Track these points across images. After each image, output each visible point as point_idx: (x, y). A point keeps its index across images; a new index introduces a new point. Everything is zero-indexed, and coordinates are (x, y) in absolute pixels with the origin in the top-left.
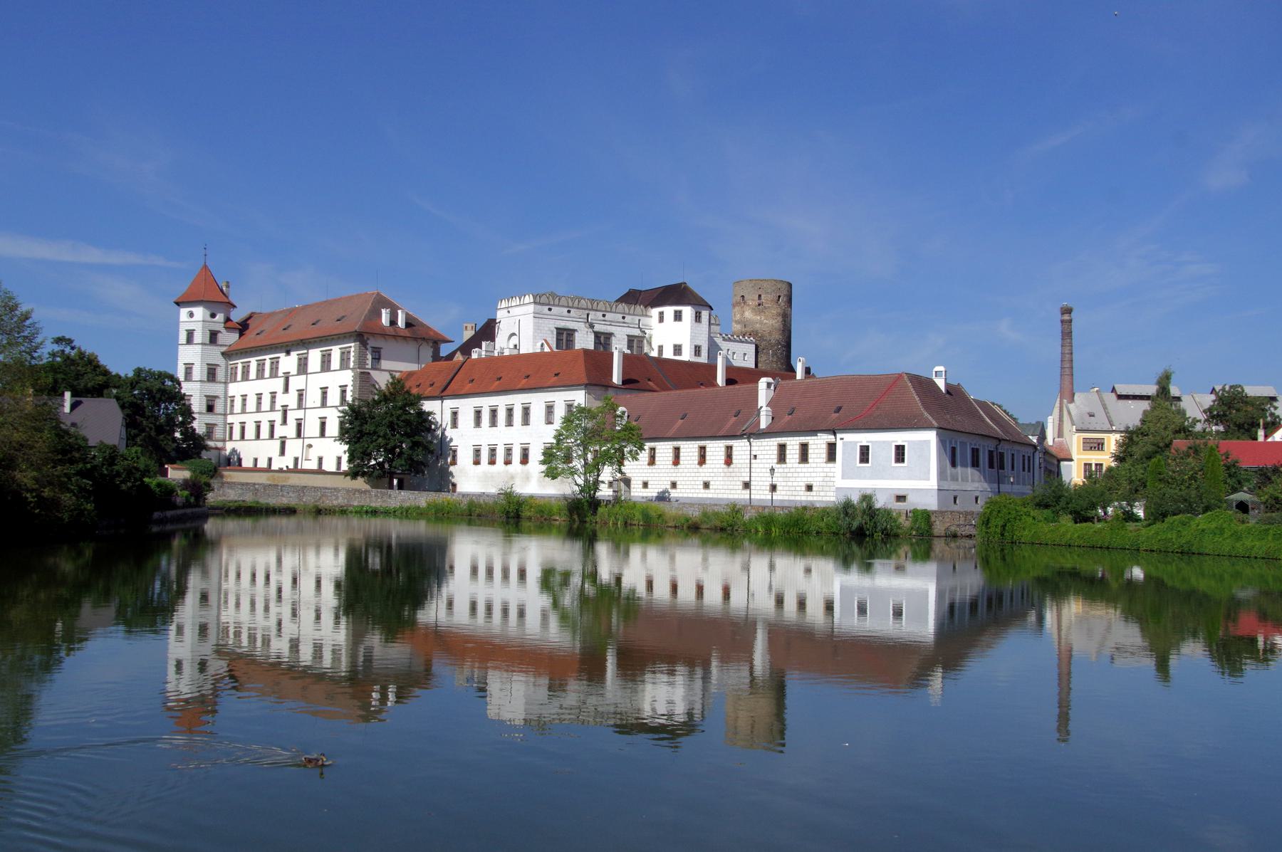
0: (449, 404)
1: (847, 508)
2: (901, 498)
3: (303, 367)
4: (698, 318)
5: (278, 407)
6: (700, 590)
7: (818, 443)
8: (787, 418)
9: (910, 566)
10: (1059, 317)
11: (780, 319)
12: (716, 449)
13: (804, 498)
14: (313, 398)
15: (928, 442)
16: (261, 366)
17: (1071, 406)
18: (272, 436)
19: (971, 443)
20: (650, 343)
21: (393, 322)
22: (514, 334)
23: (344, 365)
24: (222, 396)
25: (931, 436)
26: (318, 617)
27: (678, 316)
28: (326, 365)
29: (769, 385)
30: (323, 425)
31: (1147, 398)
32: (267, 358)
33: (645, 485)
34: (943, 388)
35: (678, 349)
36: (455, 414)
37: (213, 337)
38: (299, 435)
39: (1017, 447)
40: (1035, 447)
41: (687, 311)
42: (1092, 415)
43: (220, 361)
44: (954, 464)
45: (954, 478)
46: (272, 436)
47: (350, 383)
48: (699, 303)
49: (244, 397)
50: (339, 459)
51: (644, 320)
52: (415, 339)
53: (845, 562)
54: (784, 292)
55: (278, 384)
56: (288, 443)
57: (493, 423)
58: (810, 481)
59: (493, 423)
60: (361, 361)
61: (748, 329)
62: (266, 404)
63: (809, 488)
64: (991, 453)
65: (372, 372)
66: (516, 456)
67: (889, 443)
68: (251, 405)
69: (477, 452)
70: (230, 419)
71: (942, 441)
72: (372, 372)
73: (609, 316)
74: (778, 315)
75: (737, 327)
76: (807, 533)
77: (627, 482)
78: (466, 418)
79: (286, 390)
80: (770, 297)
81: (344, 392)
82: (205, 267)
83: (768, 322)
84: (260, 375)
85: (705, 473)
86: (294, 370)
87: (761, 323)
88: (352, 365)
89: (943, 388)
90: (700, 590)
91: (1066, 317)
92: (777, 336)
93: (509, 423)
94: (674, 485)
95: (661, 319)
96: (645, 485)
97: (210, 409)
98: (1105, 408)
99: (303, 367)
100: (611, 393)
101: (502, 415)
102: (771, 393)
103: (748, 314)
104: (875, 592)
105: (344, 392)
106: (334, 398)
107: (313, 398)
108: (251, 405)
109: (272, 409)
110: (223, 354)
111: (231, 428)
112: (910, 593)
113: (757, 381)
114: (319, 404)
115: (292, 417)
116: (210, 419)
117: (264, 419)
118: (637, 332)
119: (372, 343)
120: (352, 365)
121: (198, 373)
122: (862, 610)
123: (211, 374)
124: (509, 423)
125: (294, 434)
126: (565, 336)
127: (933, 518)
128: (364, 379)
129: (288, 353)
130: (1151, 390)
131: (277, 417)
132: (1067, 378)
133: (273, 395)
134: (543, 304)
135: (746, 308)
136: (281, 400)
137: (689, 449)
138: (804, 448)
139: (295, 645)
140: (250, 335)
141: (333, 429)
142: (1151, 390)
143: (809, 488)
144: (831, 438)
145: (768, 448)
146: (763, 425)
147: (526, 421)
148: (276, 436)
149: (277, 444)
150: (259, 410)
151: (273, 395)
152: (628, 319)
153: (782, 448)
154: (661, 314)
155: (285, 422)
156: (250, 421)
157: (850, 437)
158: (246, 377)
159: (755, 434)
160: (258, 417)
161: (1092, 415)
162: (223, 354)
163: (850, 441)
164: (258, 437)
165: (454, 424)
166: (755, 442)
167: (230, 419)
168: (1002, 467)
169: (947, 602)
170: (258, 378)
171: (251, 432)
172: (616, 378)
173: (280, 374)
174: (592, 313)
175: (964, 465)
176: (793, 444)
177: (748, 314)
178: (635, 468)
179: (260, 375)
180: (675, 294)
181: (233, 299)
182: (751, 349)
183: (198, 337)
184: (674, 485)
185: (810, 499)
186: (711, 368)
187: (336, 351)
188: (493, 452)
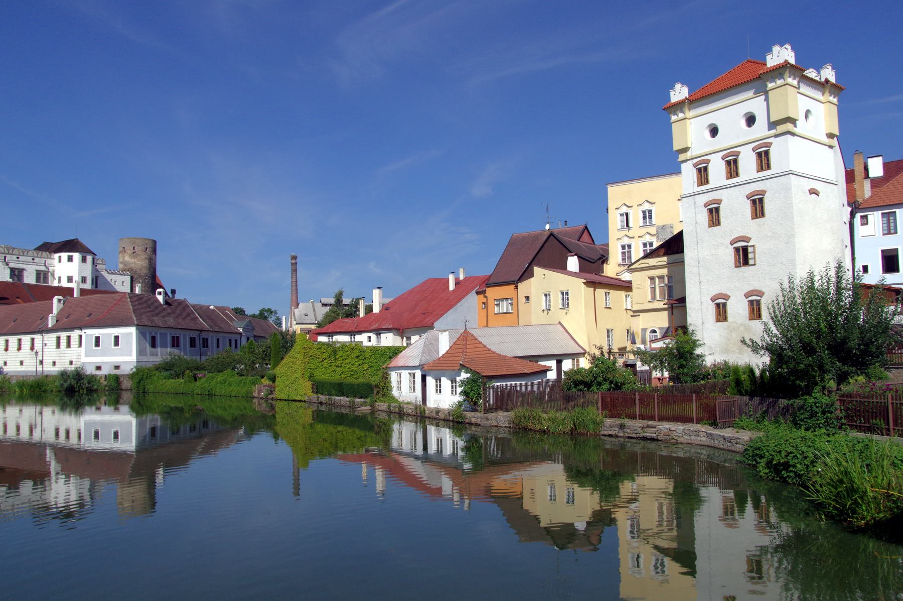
1: (64, 374)
2: (117, 367)
4: (84, 260)
6: (18, 428)
9: (105, 408)
10: (290, 261)
12: (26, 339)
15: (131, 334)
17: (296, 311)
20: (53, 275)
25: (132, 330)
27: (70, 259)
29: (59, 301)
31: (330, 305)
35: (70, 279)
39: (221, 335)
40: (241, 334)
41: (77, 256)
42: (306, 315)
44: (153, 345)
45: (152, 354)
48: (84, 251)
51: (48, 261)
53: (63, 408)
54: (150, 245)
71: (141, 334)
73: (22, 258)
75: (121, 266)
76: (45, 391)
83: (140, 263)
90: (18, 428)
91: (294, 261)
92: (145, 271)
94: (5, 363)
95: (60, 261)
98: (314, 310)
102: (61, 305)
103: (127, 258)
104: (103, 424)
112: (121, 424)
113: (52, 299)
118: (43, 268)
122: (97, 436)
127: (122, 379)
130: (332, 301)
132: (294, 295)
137: (13, 340)
138: (69, 338)
142: (332, 301)
145: (51, 338)
146: (50, 326)
152: (37, 260)
153: (59, 338)
161: (306, 315)
166: (46, 336)
169: (148, 427)
175: (164, 346)
176: (63, 335)
177: (127, 258)
180: (70, 246)
182: (127, 279)
184: (5, 363)
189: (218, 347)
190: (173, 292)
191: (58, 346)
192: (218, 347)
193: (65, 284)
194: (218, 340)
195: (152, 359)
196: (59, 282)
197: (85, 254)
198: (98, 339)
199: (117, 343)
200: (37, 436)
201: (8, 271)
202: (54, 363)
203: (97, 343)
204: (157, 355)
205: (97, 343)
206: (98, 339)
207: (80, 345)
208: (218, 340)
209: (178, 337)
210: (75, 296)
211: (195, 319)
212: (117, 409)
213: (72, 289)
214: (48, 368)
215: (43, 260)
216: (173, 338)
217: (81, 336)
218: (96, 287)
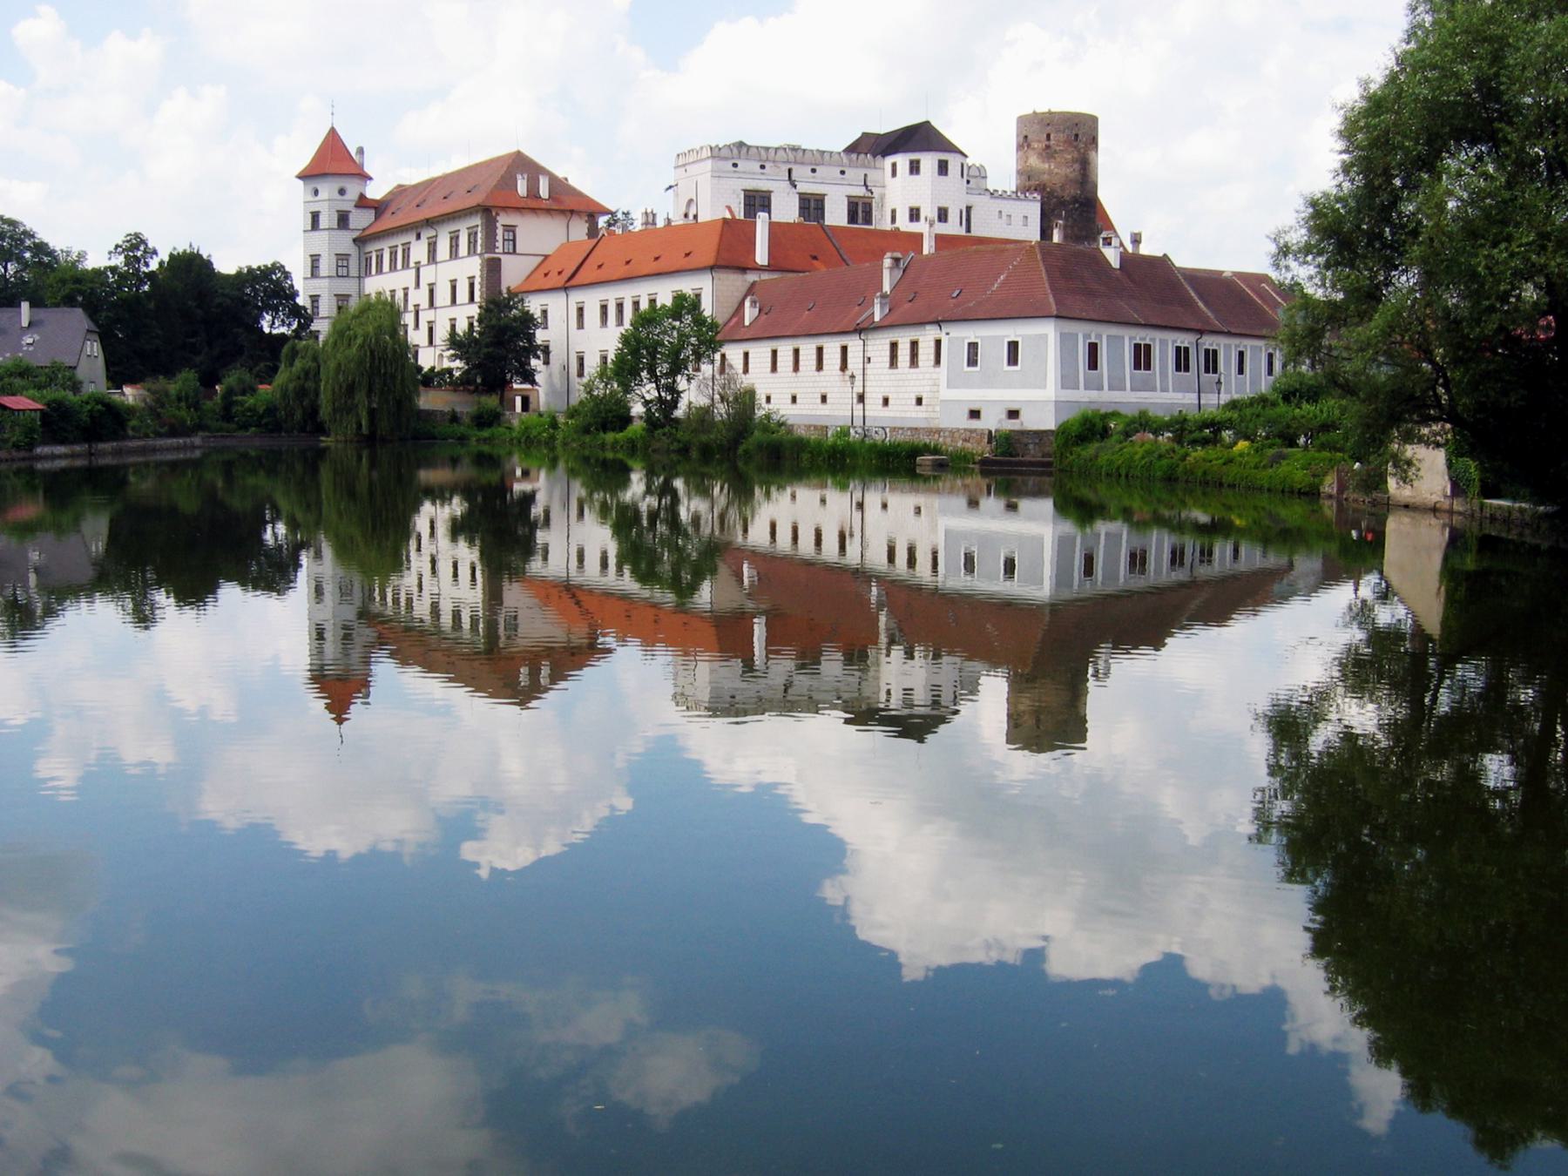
0: (576, 297)
2: (1014, 414)
4: (943, 168)
7: (927, 337)
11: (1077, 166)
12: (832, 347)
14: (443, 296)
19: (1130, 337)
21: (533, 193)
22: (691, 201)
26: (455, 575)
27: (915, 168)
28: (454, 253)
29: (897, 260)
32: (399, 241)
34: (1115, 263)
35: (915, 215)
36: (580, 311)
37: (343, 220)
41: (928, 161)
43: (352, 250)
47: (478, 274)
52: (562, 212)
55: (407, 277)
60: (490, 244)
61: (1033, 183)
63: (919, 401)
74: (1074, 161)
78: (592, 315)
80: (1062, 136)
81: (472, 286)
82: (333, 133)
84: (393, 268)
86: (424, 261)
88: (479, 250)
89: (1115, 263)
95: (894, 173)
100: (752, 277)
104: (987, 539)
105: (472, 286)
106: (463, 295)
107: (443, 296)
112: (1020, 539)
113: (882, 258)
115: (425, 317)
118: (861, 192)
119: (503, 219)
126: (757, 201)
128: (493, 269)
129: (418, 237)
134: (726, 159)
135: (1031, 152)
137: (808, 348)
138: (914, 344)
139: (435, 610)
140: (388, 215)
143: (919, 401)
145: (878, 346)
146: (877, 318)
153: (894, 346)
154: (894, 165)
155: (417, 326)
158: (380, 271)
159: (863, 329)
163: (958, 336)
165: (581, 325)
173: (412, 264)
176: (904, 339)
179: (393, 268)
181: (368, 169)
183: (324, 222)
187: (463, 228)
189: (1241, 371)
190: (1136, 240)
191: (893, 361)
192: (1241, 371)
193: (903, 224)
194: (1241, 354)
195: (1093, 395)
196: (893, 220)
197: (944, 156)
198: (973, 347)
199: (1013, 359)
200: (853, 556)
201: (795, 203)
202: (886, 401)
204: (1100, 388)
205: (972, 361)
206: (973, 347)
207: (938, 361)
208: (1241, 354)
209: (1148, 347)
210: (926, 252)
211: (1187, 303)
212: (1012, 507)
213: (918, 238)
214: (874, 409)
215: (861, 172)
216: (1137, 347)
217: (938, 343)
218: (968, 230)
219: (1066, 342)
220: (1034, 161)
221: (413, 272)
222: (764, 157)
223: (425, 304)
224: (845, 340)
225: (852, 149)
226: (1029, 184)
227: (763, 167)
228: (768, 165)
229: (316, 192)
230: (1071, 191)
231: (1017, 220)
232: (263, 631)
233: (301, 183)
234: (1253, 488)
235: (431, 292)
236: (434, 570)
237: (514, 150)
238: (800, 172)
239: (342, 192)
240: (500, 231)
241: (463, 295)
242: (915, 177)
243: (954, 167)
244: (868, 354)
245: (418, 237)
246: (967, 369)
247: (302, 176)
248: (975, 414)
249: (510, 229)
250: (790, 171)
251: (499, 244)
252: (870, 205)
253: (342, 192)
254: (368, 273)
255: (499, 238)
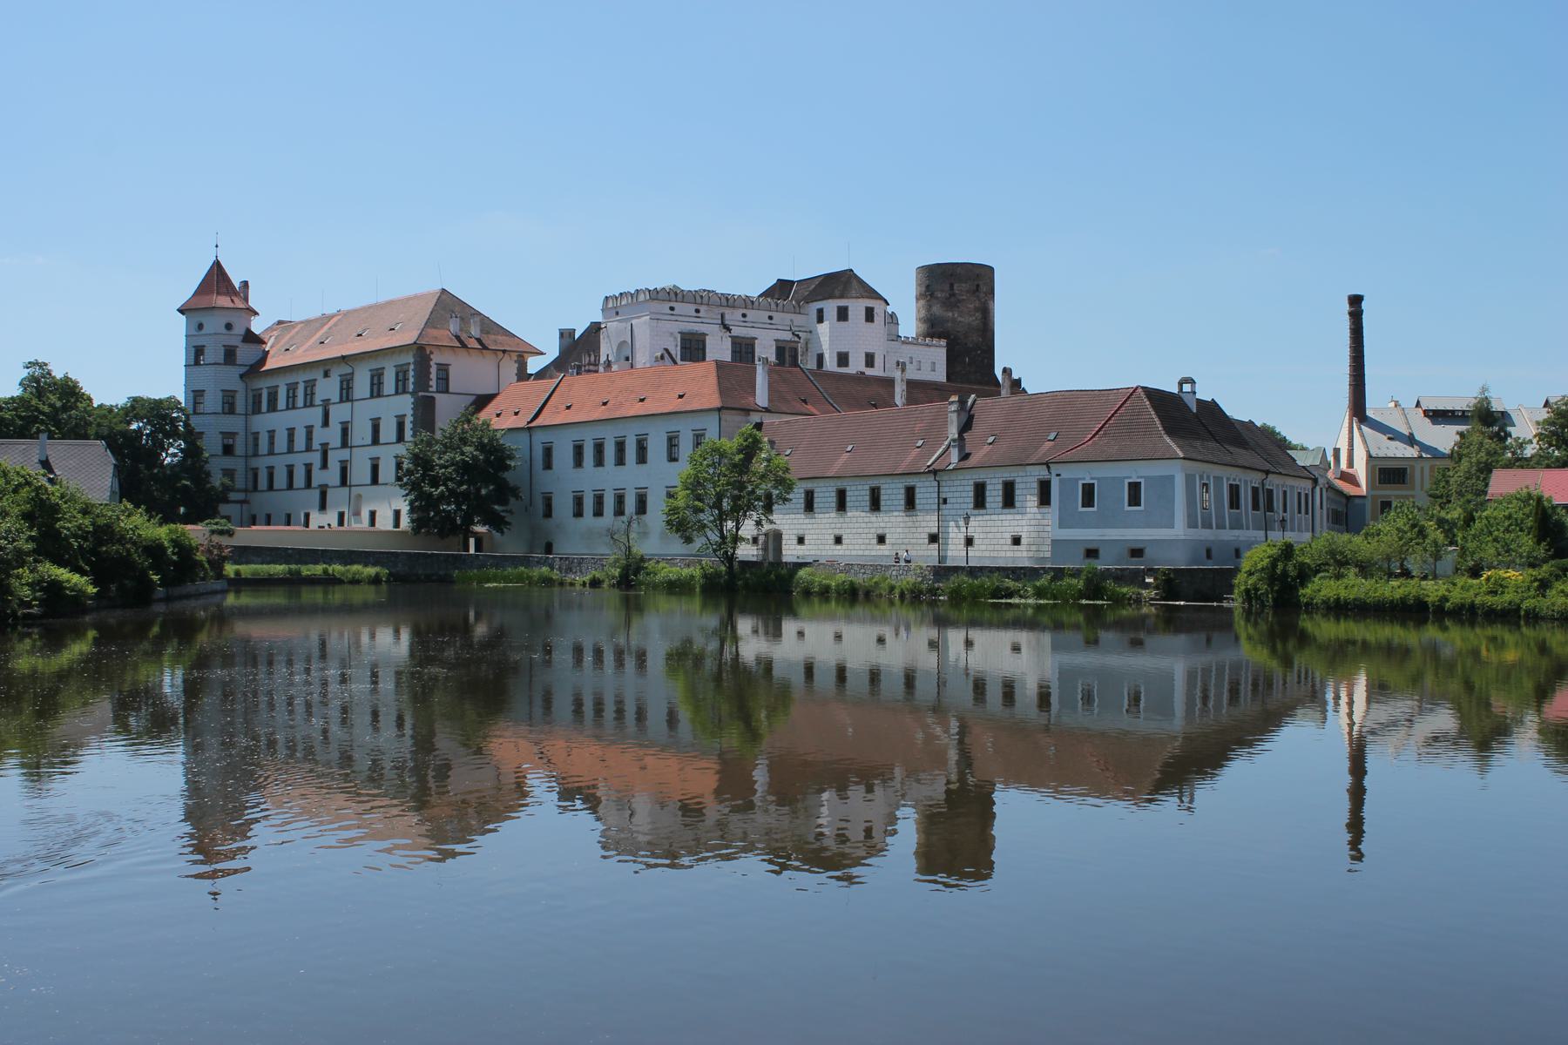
3: (346, 394)
4: (870, 315)
5: (316, 445)
8: (987, 448)
11: (978, 315)
13: (1009, 554)
14: (362, 433)
16: (292, 388)
18: (308, 485)
23: (401, 389)
24: (242, 433)
27: (843, 314)
28: (376, 391)
30: (375, 469)
33: (801, 540)
35: (843, 359)
37: (230, 355)
38: (344, 482)
41: (857, 307)
46: (308, 485)
47: (409, 412)
49: (272, 434)
50: (397, 514)
51: (798, 320)
56: (330, 493)
57: (599, 462)
58: (1017, 531)
59: (599, 462)
62: (300, 442)
63: (1016, 541)
64: (1255, 490)
65: (437, 396)
66: (630, 504)
67: (1122, 480)
68: (281, 443)
69: (579, 501)
70: (254, 463)
72: (437, 396)
74: (976, 309)
77: (777, 537)
79: (326, 423)
84: (291, 406)
85: (880, 522)
87: (954, 320)
93: (620, 461)
96: (801, 540)
97: (228, 450)
99: (346, 394)
100: (755, 418)
101: (610, 452)
106: (388, 432)
107: (362, 433)
108: (281, 443)
109: (309, 449)
110: (242, 376)
111: (256, 476)
114: (369, 440)
115: (335, 458)
116: (228, 462)
117: (299, 461)
118: (787, 336)
120: (411, 387)
121: (212, 402)
123: (229, 407)
124: (620, 461)
125: (337, 480)
129: (326, 375)
131: (315, 458)
133: (309, 431)
136: (320, 436)
141: (387, 472)
143: (1016, 541)
144: (1042, 472)
147: (642, 458)
148: (315, 483)
149: (316, 494)
150: (290, 450)
151: (309, 431)
156: (280, 464)
157: (1068, 472)
158: (273, 407)
160: (290, 459)
162: (242, 376)
164: (290, 486)
165: (548, 465)
167: (254, 463)
168: (1270, 507)
170: (288, 408)
171: (280, 480)
172: (761, 397)
173: (317, 401)
174: (727, 312)
178: (787, 521)
183: (209, 356)
185: (1018, 554)
186: (890, 382)
188: (599, 501)
198: (1088, 491)
199: (1135, 500)
201: (727, 346)
203: (1088, 499)
204: (1210, 527)
205: (1088, 499)
206: (1088, 491)
213: (890, 382)
219: (1189, 480)
220: (937, 309)
221: (319, 411)
222: (701, 299)
223: (336, 441)
224: (911, 481)
225: (766, 294)
226: (933, 328)
227: (697, 311)
228: (703, 309)
229: (200, 326)
230: (976, 338)
231: (926, 367)
232: (128, 784)
233: (183, 318)
234: (1534, 618)
235: (345, 432)
236: (344, 721)
237: (438, 288)
238: (733, 316)
239: (229, 326)
240: (433, 370)
241: (388, 432)
242: (842, 324)
243: (879, 318)
244: (943, 495)
245: (326, 375)
246: (1081, 509)
247: (181, 311)
248: (1092, 553)
249: (444, 369)
250: (723, 316)
251: (433, 383)
252: (796, 350)
253: (229, 326)
254: (257, 410)
255: (433, 376)
